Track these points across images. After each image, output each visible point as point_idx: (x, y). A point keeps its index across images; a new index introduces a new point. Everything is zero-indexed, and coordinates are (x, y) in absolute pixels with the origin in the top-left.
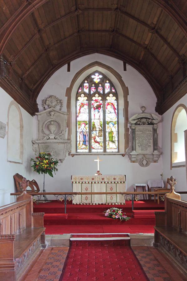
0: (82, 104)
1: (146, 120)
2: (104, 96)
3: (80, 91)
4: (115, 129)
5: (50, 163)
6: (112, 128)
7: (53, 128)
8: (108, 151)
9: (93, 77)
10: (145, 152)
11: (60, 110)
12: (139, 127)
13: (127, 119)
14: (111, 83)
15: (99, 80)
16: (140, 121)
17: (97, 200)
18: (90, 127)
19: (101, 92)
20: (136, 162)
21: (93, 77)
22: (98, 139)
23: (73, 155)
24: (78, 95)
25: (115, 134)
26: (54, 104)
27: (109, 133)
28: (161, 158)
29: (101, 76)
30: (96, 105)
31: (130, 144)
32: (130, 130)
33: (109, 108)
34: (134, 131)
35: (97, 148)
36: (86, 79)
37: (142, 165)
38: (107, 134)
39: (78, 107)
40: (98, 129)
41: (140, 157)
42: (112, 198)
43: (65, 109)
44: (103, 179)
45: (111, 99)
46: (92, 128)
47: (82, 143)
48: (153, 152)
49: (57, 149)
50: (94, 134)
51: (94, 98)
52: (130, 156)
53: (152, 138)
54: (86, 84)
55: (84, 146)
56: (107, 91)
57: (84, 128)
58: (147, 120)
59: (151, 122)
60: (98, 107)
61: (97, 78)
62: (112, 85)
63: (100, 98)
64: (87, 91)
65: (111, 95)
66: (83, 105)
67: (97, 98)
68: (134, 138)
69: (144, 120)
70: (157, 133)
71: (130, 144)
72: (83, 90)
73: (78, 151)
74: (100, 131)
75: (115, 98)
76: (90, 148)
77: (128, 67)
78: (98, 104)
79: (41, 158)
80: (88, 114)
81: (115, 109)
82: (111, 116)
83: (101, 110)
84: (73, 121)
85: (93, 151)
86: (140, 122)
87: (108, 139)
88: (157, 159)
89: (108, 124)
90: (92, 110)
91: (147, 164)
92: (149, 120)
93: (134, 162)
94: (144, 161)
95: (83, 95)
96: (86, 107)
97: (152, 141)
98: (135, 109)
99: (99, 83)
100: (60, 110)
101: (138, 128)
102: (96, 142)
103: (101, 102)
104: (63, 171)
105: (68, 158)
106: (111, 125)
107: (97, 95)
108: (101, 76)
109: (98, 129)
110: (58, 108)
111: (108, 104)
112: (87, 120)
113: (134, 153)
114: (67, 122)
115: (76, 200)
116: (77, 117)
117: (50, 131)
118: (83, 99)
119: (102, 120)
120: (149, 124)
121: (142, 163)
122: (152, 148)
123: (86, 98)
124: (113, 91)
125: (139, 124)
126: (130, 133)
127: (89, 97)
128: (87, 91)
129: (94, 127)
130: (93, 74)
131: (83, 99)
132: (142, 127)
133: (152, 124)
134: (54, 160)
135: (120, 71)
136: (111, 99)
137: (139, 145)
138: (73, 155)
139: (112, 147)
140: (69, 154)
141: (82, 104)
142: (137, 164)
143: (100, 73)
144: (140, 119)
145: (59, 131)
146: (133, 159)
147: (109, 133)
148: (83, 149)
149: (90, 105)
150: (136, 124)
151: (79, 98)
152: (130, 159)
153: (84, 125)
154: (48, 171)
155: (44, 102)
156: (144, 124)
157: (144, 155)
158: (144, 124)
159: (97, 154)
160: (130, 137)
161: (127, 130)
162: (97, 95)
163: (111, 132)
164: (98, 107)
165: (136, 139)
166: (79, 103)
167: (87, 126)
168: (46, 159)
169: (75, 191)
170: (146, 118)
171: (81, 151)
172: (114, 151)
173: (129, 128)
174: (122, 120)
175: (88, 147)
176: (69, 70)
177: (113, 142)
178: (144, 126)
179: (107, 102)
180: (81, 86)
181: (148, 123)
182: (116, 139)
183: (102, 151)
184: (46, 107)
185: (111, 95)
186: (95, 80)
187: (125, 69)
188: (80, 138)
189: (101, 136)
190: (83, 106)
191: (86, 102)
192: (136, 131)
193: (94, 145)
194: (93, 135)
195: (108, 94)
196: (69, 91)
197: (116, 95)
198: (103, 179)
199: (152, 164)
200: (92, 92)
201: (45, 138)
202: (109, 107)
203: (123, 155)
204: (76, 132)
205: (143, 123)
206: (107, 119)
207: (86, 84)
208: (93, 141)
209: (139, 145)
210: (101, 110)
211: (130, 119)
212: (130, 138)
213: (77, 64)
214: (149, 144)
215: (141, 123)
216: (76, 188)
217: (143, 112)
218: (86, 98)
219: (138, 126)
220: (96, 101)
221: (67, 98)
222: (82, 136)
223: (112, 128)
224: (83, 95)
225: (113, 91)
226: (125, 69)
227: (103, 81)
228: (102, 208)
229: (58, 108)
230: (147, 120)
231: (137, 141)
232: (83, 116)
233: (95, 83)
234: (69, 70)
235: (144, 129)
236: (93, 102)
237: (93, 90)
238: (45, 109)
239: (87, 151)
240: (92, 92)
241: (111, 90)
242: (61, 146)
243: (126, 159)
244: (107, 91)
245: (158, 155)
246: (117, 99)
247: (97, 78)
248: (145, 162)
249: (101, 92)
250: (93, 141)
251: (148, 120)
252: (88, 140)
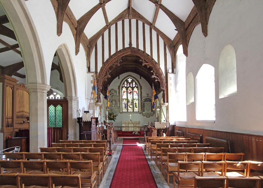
0: (124, 91)
2: (133, 88)
3: (123, 86)
4: (137, 102)
5: (113, 117)
6: (136, 102)
7: (114, 102)
8: (135, 111)
9: (128, 80)
10: (148, 112)
11: (116, 95)
13: (141, 99)
14: (135, 82)
15: (131, 81)
16: (146, 100)
17: (131, 129)
18: (127, 101)
19: (132, 86)
21: (128, 80)
22: (131, 106)
23: (121, 113)
24: (122, 87)
25: (137, 104)
26: (114, 93)
27: (135, 104)
28: (154, 115)
29: (131, 80)
30: (129, 92)
31: (143, 109)
32: (143, 103)
33: (135, 93)
34: (144, 104)
35: (130, 110)
36: (125, 81)
37: (147, 117)
38: (134, 104)
39: (123, 93)
40: (130, 102)
41: (146, 114)
42: (135, 129)
43: (118, 94)
44: (132, 122)
45: (136, 89)
46: (128, 101)
47: (124, 107)
49: (115, 110)
50: (129, 104)
51: (129, 89)
52: (142, 114)
54: (126, 83)
55: (125, 109)
56: (134, 86)
57: (125, 102)
60: (130, 93)
61: (130, 80)
62: (136, 84)
63: (131, 89)
64: (126, 86)
65: (135, 88)
66: (124, 92)
67: (130, 89)
68: (144, 107)
69: (148, 99)
71: (143, 109)
72: (124, 85)
73: (123, 111)
74: (131, 103)
75: (137, 89)
76: (128, 110)
77: (142, 78)
78: (130, 91)
79: (110, 114)
80: (126, 96)
81: (137, 94)
82: (136, 97)
83: (132, 94)
84: (121, 98)
85: (129, 111)
87: (134, 106)
89: (135, 100)
90: (128, 94)
91: (149, 117)
93: (144, 116)
94: (148, 116)
95: (124, 88)
96: (126, 93)
97: (151, 108)
98: (144, 95)
99: (131, 82)
100: (116, 95)
101: (145, 103)
102: (130, 107)
103: (132, 91)
104: (118, 119)
105: (119, 114)
106: (136, 100)
107: (130, 88)
108: (131, 80)
109: (130, 102)
110: (115, 94)
111: (134, 92)
112: (126, 98)
113: (144, 112)
114: (120, 100)
115: (124, 130)
116: (122, 97)
117: (112, 103)
118: (124, 89)
119: (132, 98)
120: (150, 101)
122: (151, 111)
123: (126, 89)
124: (136, 86)
125: (146, 101)
127: (127, 88)
128: (126, 86)
129: (129, 101)
130: (128, 78)
131: (124, 89)
134: (115, 115)
135: (139, 79)
136: (136, 89)
138: (121, 113)
139: (136, 109)
140: (120, 113)
141: (124, 91)
142: (145, 117)
143: (131, 78)
145: (116, 104)
146: (144, 115)
147: (135, 104)
148: (125, 110)
149: (127, 92)
150: (145, 101)
151: (123, 89)
152: (143, 115)
153: (125, 100)
154: (113, 119)
155: (110, 91)
158: (148, 101)
159: (130, 113)
160: (143, 106)
161: (141, 103)
162: (130, 88)
163: (136, 104)
164: (130, 93)
166: (123, 91)
167: (126, 100)
168: (112, 115)
169: (123, 126)
170: (149, 99)
171: (124, 111)
172: (137, 111)
174: (140, 99)
175: (127, 109)
176: (119, 79)
177: (137, 107)
179: (134, 91)
180: (124, 83)
182: (138, 106)
183: (132, 111)
184: (111, 93)
185: (135, 88)
186: (129, 81)
187: (141, 79)
188: (124, 106)
189: (132, 105)
190: (124, 92)
191: (126, 91)
193: (129, 109)
194: (128, 104)
195: (134, 87)
196: (119, 87)
197: (137, 87)
198: (132, 122)
199: (151, 117)
200: (128, 86)
201: (111, 107)
202: (135, 93)
203: (140, 113)
204: (122, 103)
206: (134, 98)
207: (126, 83)
208: (128, 107)
210: (132, 94)
211: (142, 99)
212: (142, 107)
213: (122, 76)
216: (123, 125)
217: (148, 96)
218: (126, 89)
220: (130, 90)
221: (118, 90)
222: (124, 105)
223: (136, 102)
224: (124, 88)
225: (136, 86)
226: (141, 79)
227: (132, 82)
228: (132, 132)
229: (115, 94)
231: (145, 108)
232: (125, 97)
233: (129, 82)
234: (119, 79)
236: (128, 90)
237: (128, 86)
238: (110, 95)
239: (126, 111)
240: (128, 86)
241: (135, 85)
242: (117, 109)
243: (141, 115)
244: (134, 86)
246: (138, 90)
247: (130, 80)
248: (148, 116)
249: (132, 86)
250: (128, 107)
252: (127, 106)
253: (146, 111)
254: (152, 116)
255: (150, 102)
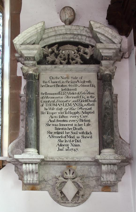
1: (75, 48)
10: (71, 156)
12: (51, 70)
16: (54, 53)
20: (41, 189)
31: (22, 131)
32: (24, 83)
34: (33, 81)
41: (55, 171)
48: (100, 153)
53: (95, 108)
58: (78, 51)
59: (92, 56)
69: (71, 51)
70: (111, 93)
86: (56, 55)
88: (112, 178)
91: (79, 197)
92: (87, 50)
93: (33, 187)
97: (94, 118)
101: (47, 73)
120: (85, 62)
121: (62, 193)
122: (95, 141)
125: (53, 63)
126: (22, 92)
132: (61, 70)
133: (95, 60)
137: (52, 129)
144: (55, 48)
146: (29, 179)
150: (42, 60)
152: (21, 178)
156: (69, 63)
157: (68, 164)
158: (69, 61)
165: (42, 109)
173: (21, 77)
178: (69, 66)
181: (82, 58)
192: (41, 83)
199: (97, 197)
205: (64, 59)
209: (52, 129)
214: (86, 129)
215: (57, 60)
219: (49, 66)
230: (78, 51)
231: (44, 119)
235: (68, 78)
245: (114, 164)
248: (70, 190)
251: (82, 48)
253: (50, 148)
254: (108, 187)
255: (89, 73)
